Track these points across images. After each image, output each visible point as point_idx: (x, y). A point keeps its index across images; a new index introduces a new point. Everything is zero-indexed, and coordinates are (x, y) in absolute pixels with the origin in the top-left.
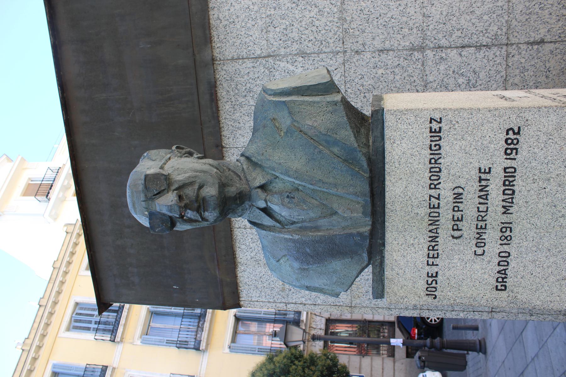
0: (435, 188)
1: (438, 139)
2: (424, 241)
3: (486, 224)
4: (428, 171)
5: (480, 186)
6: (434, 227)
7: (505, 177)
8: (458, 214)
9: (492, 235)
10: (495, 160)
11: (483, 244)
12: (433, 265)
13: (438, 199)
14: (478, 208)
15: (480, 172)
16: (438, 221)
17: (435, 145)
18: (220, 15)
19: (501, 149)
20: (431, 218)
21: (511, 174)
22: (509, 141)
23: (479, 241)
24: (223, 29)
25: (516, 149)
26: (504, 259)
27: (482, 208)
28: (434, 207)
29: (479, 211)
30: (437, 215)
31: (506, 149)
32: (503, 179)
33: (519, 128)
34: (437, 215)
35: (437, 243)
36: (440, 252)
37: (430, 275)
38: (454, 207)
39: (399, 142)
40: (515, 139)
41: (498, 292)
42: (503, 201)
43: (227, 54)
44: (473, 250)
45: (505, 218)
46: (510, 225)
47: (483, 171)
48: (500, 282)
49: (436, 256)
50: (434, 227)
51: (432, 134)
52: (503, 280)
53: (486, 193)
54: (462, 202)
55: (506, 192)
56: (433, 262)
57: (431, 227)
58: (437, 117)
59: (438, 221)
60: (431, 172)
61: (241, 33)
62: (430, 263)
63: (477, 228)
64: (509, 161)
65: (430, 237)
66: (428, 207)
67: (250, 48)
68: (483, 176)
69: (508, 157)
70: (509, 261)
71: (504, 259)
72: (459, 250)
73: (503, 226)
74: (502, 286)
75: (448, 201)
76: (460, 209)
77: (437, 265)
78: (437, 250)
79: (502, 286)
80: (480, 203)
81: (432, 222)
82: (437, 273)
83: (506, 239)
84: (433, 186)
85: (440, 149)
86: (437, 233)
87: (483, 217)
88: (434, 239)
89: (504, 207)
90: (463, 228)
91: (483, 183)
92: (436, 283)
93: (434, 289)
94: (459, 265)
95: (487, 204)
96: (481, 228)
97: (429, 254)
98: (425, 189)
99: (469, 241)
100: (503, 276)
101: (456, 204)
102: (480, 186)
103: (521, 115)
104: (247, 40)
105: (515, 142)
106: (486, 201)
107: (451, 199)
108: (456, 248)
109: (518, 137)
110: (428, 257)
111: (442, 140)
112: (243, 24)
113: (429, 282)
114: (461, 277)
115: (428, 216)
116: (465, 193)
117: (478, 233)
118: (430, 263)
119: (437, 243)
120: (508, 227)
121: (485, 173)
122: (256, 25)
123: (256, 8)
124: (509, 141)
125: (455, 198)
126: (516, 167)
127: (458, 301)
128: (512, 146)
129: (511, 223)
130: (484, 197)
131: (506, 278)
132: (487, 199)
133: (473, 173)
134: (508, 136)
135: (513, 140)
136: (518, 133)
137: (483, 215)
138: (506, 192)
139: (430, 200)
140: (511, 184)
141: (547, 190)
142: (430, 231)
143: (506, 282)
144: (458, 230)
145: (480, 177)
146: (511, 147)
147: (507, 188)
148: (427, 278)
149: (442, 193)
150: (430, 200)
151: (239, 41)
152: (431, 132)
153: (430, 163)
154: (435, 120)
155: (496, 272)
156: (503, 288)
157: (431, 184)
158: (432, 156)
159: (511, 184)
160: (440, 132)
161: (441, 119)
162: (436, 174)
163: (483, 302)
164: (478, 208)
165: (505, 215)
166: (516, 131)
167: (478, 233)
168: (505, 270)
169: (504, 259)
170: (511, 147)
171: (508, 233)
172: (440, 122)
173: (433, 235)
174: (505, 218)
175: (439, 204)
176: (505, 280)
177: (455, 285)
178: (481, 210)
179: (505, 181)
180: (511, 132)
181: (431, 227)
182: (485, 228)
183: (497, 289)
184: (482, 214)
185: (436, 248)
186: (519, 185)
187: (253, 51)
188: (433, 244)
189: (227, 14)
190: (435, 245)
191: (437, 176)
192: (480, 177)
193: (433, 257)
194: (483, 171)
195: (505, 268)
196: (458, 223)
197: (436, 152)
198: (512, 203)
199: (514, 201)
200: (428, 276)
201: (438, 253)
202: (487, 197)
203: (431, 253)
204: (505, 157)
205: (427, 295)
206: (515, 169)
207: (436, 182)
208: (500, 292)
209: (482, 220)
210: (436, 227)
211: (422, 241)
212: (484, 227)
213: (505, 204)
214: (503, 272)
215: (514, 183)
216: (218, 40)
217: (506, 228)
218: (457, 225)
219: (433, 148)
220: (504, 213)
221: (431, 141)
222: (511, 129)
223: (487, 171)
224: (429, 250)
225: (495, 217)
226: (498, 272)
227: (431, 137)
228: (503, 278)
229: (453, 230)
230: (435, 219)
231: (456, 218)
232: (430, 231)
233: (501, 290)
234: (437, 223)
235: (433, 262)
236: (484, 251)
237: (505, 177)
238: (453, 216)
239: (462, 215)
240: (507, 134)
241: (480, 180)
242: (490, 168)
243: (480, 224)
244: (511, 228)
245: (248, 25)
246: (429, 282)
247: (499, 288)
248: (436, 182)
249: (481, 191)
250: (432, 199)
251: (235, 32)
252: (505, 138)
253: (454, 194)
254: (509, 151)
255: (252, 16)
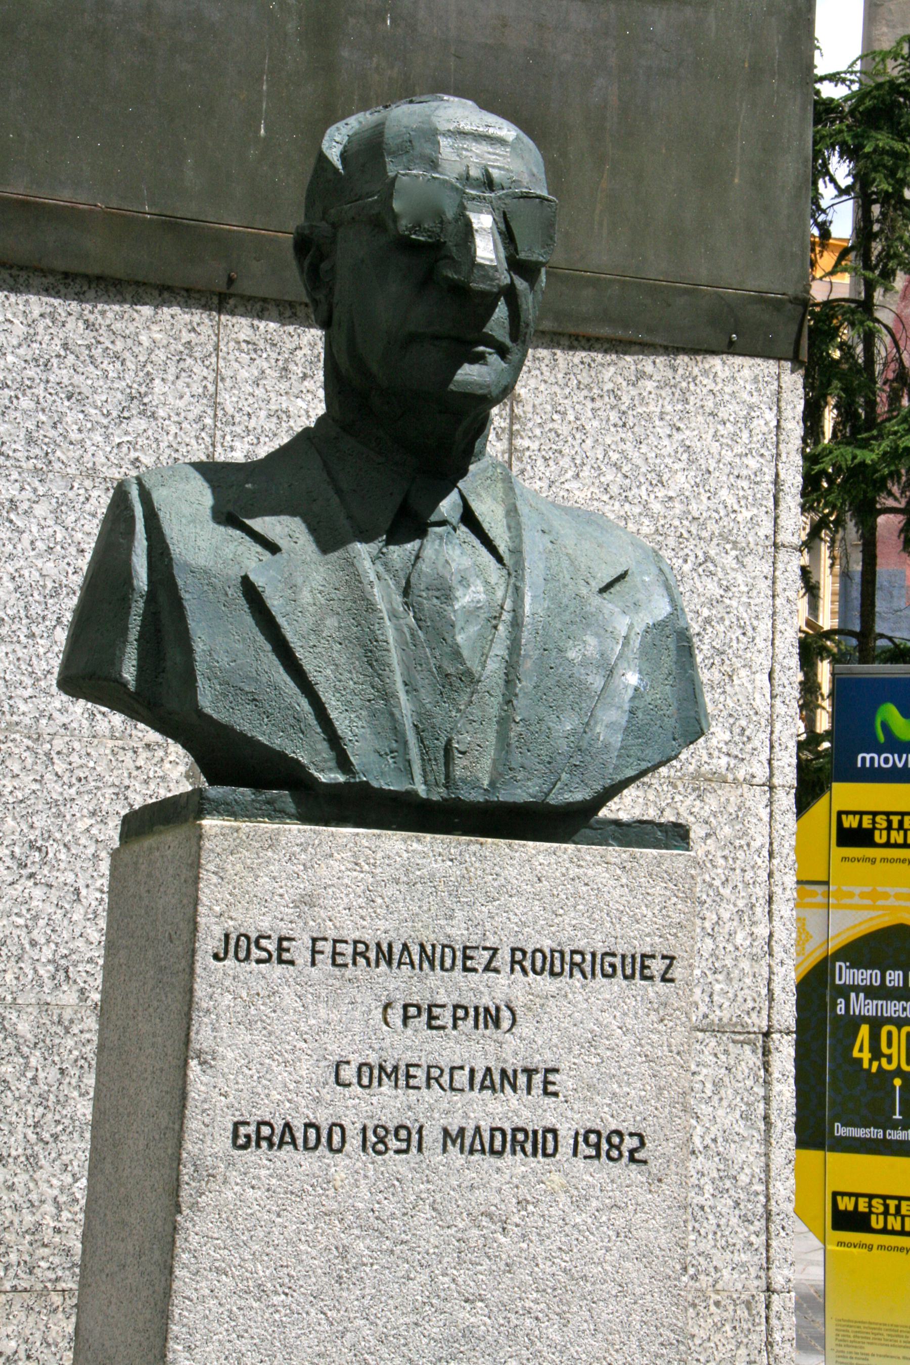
0: (513, 962)
1: (628, 971)
2: (379, 929)
3: (418, 1088)
4: (554, 946)
5: (515, 1071)
6: (416, 958)
7: (535, 1132)
8: (446, 1018)
9: (388, 1104)
10: (576, 1107)
11: (365, 1081)
12: (314, 952)
13: (487, 969)
14: (462, 1068)
15: (547, 1071)
16: (432, 967)
17: (613, 966)
18: (650, 385)
19: (598, 1120)
20: (438, 950)
21: (540, 1146)
22: (616, 1140)
23: (376, 1072)
24: (610, 386)
25: (598, 1156)
26: (325, 1138)
27: (462, 1078)
28: (466, 958)
29: (452, 1069)
30: (448, 964)
31: (598, 1134)
32: (530, 1129)
33: (645, 1162)
34: (448, 964)
35: (373, 964)
36: (349, 972)
37: (285, 944)
38: (466, 1009)
39: (624, 881)
40: (621, 1155)
41: (230, 1127)
42: (478, 1129)
43: (532, 383)
44: (351, 1057)
45: (432, 1136)
46: (414, 1150)
47: (551, 1077)
48: (258, 1131)
49: (339, 960)
50: (416, 958)
51: (638, 960)
52: (265, 1138)
53: (498, 1086)
54: (476, 1026)
55: (498, 1136)
56: (322, 952)
57: (415, 950)
58: (677, 972)
59: (432, 967)
60: (552, 951)
61: (589, 442)
62: (320, 945)
63: (408, 1066)
64: (572, 1141)
65: (390, 946)
66: (468, 944)
67: (540, 462)
68: (538, 1079)
69: (581, 1139)
70: (317, 1153)
71: (325, 1138)
72: (352, 1021)
73: (414, 1132)
74: (248, 1136)
75: (481, 993)
76: (460, 1022)
77: (313, 964)
78: (355, 963)
79: (248, 1136)
80: (472, 1071)
81: (429, 952)
82: (292, 963)
83: (377, 1139)
84: (519, 959)
85: (605, 975)
86: (400, 963)
87: (437, 1080)
88: (385, 955)
89: (462, 1131)
90: (409, 1032)
91: (522, 1079)
92: (259, 961)
93: (242, 955)
94: (312, 1021)
95: (472, 1088)
96: (409, 1076)
97: (346, 942)
98: (512, 939)
99: (376, 1046)
100: (276, 1140)
101: (472, 1012)
102: (515, 1071)
103: (673, 1167)
104: (565, 462)
105: (615, 1153)
106: (477, 1086)
107: (486, 1001)
108: (357, 1014)
109: (625, 1160)
110: (335, 941)
111: (625, 983)
112: (615, 456)
113: (264, 942)
114: (277, 1028)
115: (446, 942)
116: (498, 1035)
117: (396, 1068)
118: (320, 945)
119: (373, 964)
120: (409, 1145)
121: (546, 1082)
122: (605, 498)
123: (656, 507)
124: (616, 1140)
125: (487, 1010)
126: (558, 1156)
127: (206, 1020)
128: (605, 1146)
129: (420, 1149)
130: (487, 1083)
131: (271, 1145)
132: (483, 1088)
133: (548, 1055)
134: (627, 1138)
135: (618, 1148)
136: (632, 1159)
137: (442, 1080)
138: (498, 1136)
139: (485, 948)
140: (518, 1148)
141: (499, 1236)
142: (405, 947)
143: (258, 1146)
144: (406, 1018)
145: (536, 1071)
146: (601, 1144)
147: (509, 1138)
148: (275, 937)
149: (502, 979)
150: (485, 948)
151: (564, 430)
152: (644, 956)
153: (573, 952)
154: (669, 966)
155: (289, 1118)
156: (242, 1141)
157: (524, 953)
158: (588, 957)
159: (518, 1148)
160: (644, 978)
161: (672, 980)
162: (548, 966)
163: (203, 1088)
164: (462, 1068)
165: (441, 1137)
166: (636, 1155)
167: (396, 1068)
168: (294, 1142)
169: (324, 1140)
170: (601, 1144)
171: (394, 1144)
172: (664, 979)
173: (396, 957)
174: (432, 1136)
175: (474, 970)
176: (264, 1144)
177: (253, 1011)
178: (457, 1074)
179: (525, 1131)
180: (634, 1142)
181: (415, 950)
182: (408, 1086)
183: (236, 1125)
184: (446, 1077)
185: (361, 961)
186: (516, 1165)
187: (529, 473)
188: (372, 955)
189: (652, 408)
190: (368, 959)
191: (543, 969)
192: (536, 1071)
193: (335, 954)
194: (551, 1077)
195: (300, 1142)
196: (425, 1017)
197: (598, 967)
198: (472, 1152)
199: (477, 1157)
200: (281, 940)
201: (346, 965)
202: (487, 1088)
203: (348, 949)
204: (582, 1131)
205: (227, 936)
206: (553, 1155)
207: (527, 964)
208: (229, 1134)
209: (429, 1078)
210: (417, 962)
211: (382, 924)
212: (412, 1082)
213: (469, 1133)
214: (288, 1139)
215: (520, 1155)
216: (576, 360)
217: (408, 1140)
218: (419, 1015)
219: (608, 959)
220: (446, 1132)
221: (624, 957)
222: (643, 1144)
223: (551, 1088)
224: (356, 942)
225: (436, 1109)
226: (287, 1125)
227: (633, 957)
228: (269, 1139)
229: (406, 1007)
230: (437, 963)
231: (436, 1011)
232: (405, 947)
233: (236, 1135)
234: (426, 965)
235: (322, 952)
236: (349, 1085)
237: (535, 1132)
238: (443, 1006)
239: (443, 1028)
240: (631, 1135)
241: (530, 1072)
242: (556, 1094)
243: (421, 1074)
244: (406, 1151)
245: (609, 476)
246: (264, 942)
247: (242, 1130)
248: (527, 964)
249: (503, 1072)
250: (487, 955)
251: (596, 423)
252: (624, 1131)
253: (498, 1009)
254: (593, 1138)
255: (635, 491)
